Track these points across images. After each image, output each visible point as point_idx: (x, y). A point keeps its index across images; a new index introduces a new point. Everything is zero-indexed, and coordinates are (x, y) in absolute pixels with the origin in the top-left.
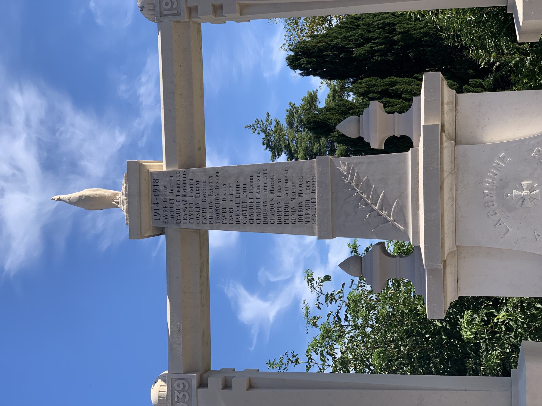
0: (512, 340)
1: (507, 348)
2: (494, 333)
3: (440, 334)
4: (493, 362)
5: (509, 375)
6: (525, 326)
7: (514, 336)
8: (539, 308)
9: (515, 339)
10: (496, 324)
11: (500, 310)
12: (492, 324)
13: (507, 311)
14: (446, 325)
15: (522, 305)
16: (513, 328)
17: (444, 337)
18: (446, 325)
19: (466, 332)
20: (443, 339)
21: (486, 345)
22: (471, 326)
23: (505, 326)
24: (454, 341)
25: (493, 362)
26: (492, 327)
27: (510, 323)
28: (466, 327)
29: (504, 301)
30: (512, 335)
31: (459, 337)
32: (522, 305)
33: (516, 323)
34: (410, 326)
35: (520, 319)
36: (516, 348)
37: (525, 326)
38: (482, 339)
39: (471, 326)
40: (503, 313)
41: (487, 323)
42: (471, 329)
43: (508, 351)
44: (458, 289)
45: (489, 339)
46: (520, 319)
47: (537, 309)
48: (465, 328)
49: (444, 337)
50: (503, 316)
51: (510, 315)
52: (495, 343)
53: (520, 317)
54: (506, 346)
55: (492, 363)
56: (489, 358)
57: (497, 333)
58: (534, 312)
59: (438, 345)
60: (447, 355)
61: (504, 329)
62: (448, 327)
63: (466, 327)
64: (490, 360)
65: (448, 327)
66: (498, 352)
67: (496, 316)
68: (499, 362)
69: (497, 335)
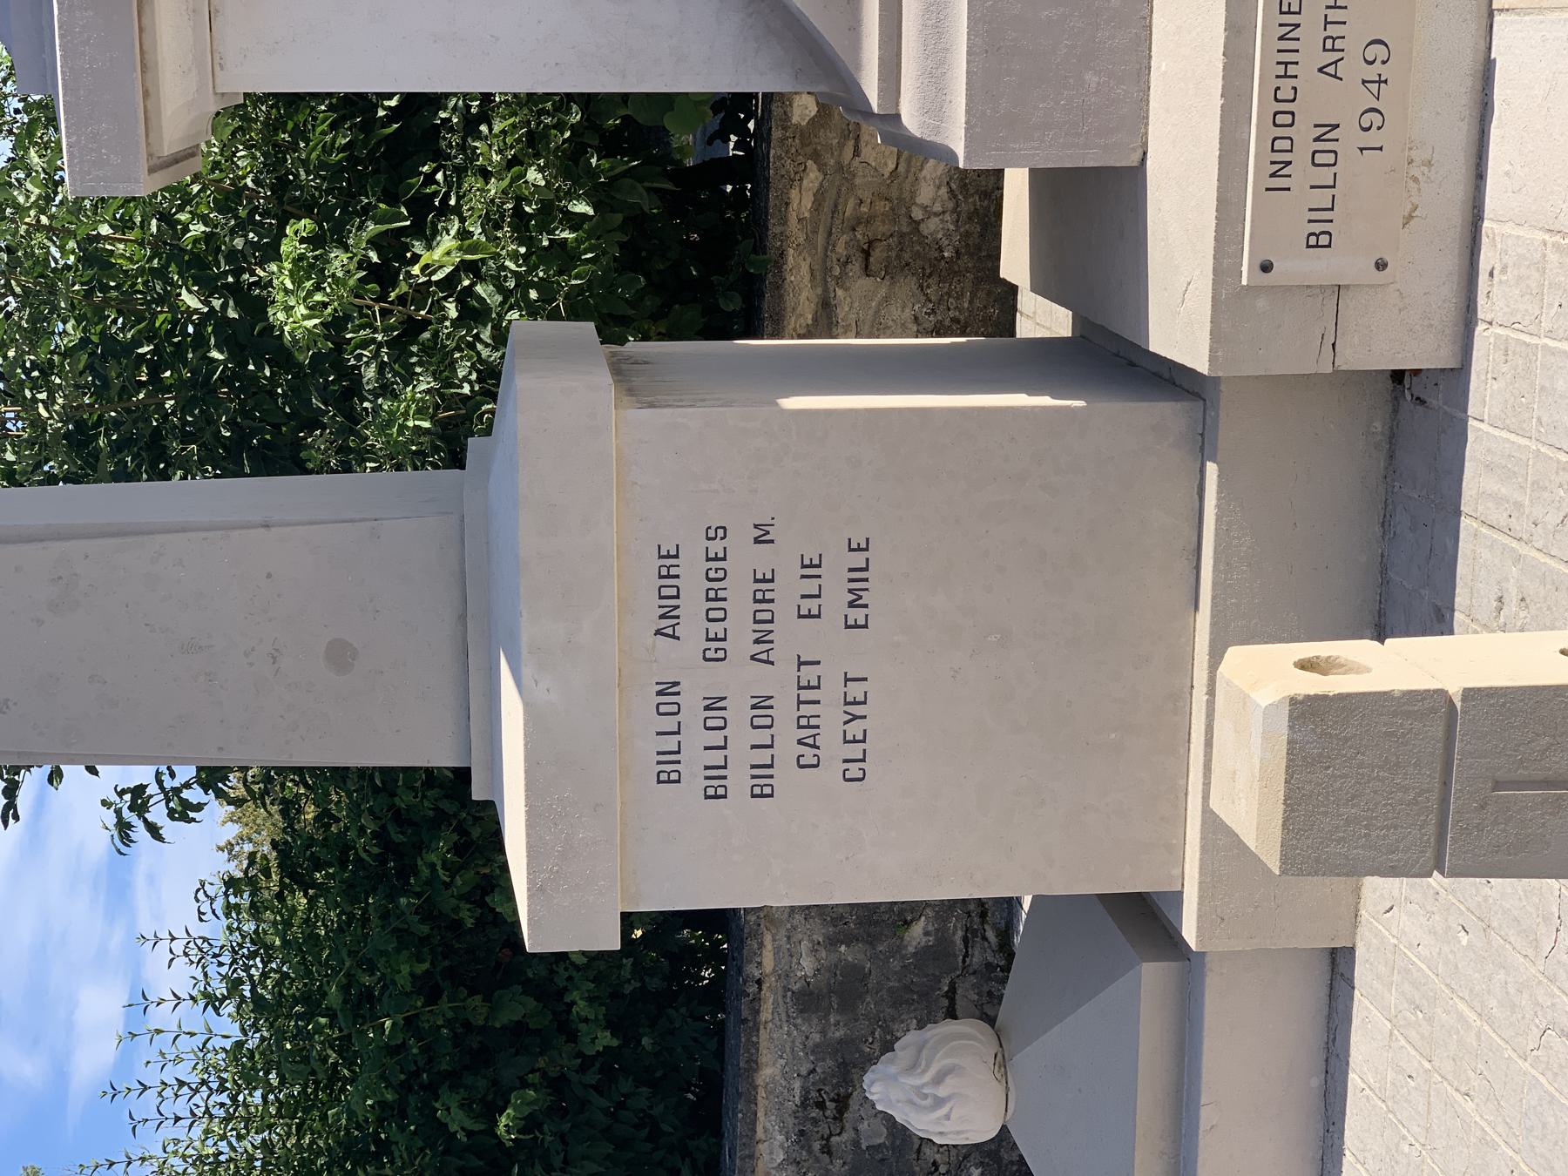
0: (485, 353)
1: (465, 379)
2: (412, 328)
3: (200, 342)
4: (402, 427)
5: (457, 460)
6: (533, 295)
7: (493, 337)
8: (584, 216)
9: (495, 349)
10: (421, 291)
11: (435, 232)
12: (403, 288)
13: (464, 234)
14: (224, 306)
15: (518, 212)
16: (489, 309)
17: (215, 354)
18: (224, 306)
19: (288, 309)
20: (213, 360)
21: (381, 367)
22: (308, 284)
23: (461, 302)
24: (260, 368)
25: (402, 427)
26: (402, 299)
27: (479, 289)
28: (290, 286)
29: (452, 202)
30: (486, 334)
31: (268, 344)
32: (518, 210)
33: (500, 289)
34: (64, 309)
35: (512, 266)
36: (490, 377)
37: (533, 295)
38: (364, 344)
39: (308, 284)
40: (447, 242)
41: (382, 275)
42: (310, 294)
43: (466, 389)
44: (216, 63)
45: (389, 344)
46: (512, 266)
47: (575, 221)
48: (286, 291)
49: (215, 354)
50: (448, 253)
51: (473, 249)
52: (420, 363)
53: (514, 256)
54: (461, 373)
55: (400, 433)
56: (391, 413)
57: (425, 323)
58: (565, 235)
59: (199, 390)
60: (230, 424)
61: (453, 314)
62: (232, 314)
63: (290, 286)
64: (390, 423)
65: (232, 314)
66: (423, 387)
67: (416, 258)
68: (426, 424)
69: (426, 335)
